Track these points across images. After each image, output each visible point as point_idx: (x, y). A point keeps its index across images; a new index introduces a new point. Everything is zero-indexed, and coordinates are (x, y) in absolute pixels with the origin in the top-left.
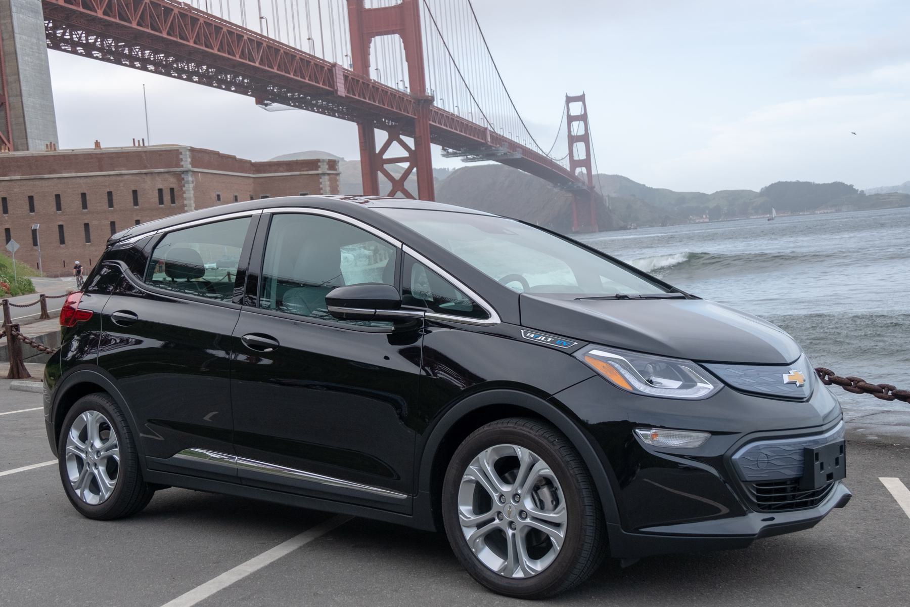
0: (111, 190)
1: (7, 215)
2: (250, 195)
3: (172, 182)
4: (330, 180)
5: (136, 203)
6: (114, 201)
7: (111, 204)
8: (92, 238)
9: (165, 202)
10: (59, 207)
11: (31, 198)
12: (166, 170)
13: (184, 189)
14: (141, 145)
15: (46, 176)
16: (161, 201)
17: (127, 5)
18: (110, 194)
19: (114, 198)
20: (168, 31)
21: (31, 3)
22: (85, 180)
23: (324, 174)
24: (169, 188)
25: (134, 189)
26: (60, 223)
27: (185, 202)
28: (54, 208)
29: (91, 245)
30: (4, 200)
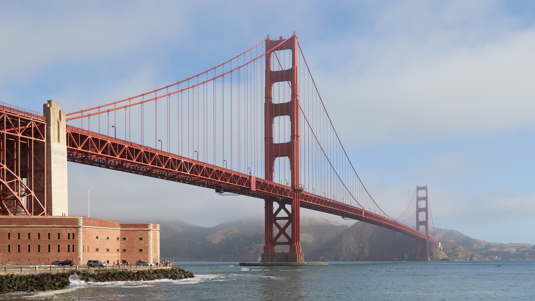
3: (74, 231)
4: (153, 233)
5: (59, 238)
6: (50, 237)
7: (49, 238)
8: (40, 250)
10: (29, 239)
11: (19, 234)
14: (64, 215)
16: (69, 238)
18: (49, 234)
19: (50, 235)
26: (29, 244)
27: (78, 239)
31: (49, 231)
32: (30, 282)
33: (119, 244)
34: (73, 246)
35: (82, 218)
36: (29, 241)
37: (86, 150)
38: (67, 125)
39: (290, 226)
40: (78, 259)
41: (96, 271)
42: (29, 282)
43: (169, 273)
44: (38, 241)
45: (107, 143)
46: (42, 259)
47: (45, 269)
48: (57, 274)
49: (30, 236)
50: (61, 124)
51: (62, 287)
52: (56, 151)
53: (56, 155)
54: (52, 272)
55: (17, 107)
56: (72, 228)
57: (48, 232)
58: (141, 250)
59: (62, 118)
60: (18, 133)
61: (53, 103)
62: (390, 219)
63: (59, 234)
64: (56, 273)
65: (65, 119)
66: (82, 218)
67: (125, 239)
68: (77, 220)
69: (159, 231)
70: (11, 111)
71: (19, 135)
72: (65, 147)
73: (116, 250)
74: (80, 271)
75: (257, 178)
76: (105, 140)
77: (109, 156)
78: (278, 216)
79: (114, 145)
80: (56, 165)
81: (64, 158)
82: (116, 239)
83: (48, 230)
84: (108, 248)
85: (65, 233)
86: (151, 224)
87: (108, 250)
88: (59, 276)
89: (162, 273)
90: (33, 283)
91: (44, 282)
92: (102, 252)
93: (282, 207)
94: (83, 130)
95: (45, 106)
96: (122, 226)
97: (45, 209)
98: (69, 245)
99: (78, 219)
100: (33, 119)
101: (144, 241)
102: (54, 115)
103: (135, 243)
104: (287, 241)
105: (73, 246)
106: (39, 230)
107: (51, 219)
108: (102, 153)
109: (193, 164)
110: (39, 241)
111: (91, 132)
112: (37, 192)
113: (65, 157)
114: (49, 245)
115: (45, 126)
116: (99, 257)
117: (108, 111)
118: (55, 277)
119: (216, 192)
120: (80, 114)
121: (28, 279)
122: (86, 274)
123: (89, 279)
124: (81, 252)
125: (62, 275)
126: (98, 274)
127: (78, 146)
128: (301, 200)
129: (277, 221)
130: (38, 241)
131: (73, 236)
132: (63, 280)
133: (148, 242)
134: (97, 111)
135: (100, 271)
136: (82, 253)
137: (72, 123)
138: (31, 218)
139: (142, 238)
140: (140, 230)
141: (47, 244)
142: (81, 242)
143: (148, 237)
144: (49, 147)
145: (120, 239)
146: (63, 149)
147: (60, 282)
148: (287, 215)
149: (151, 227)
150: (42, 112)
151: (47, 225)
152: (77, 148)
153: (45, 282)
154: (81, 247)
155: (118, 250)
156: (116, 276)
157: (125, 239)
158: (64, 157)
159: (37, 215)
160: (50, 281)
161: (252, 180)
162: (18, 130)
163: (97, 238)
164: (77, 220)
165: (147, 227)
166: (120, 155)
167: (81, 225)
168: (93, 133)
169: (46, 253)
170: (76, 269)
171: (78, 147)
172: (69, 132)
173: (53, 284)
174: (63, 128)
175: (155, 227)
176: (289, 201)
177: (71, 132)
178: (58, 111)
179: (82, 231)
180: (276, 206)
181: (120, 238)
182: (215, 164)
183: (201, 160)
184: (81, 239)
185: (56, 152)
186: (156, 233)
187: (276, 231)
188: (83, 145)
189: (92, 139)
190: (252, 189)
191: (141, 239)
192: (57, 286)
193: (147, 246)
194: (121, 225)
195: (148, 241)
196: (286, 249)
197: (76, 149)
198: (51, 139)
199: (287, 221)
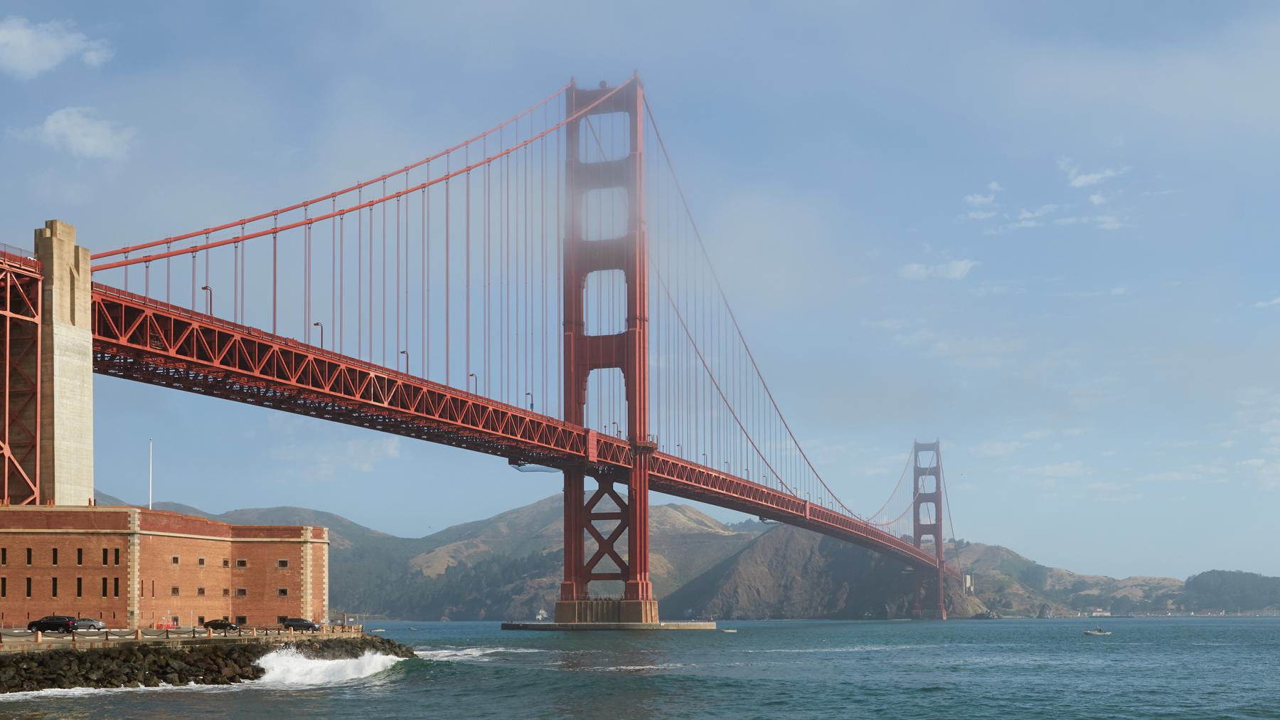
3: (117, 542)
5: (80, 562)
6: (58, 558)
7: (55, 562)
8: (32, 592)
9: (109, 562)
12: (112, 531)
13: (129, 550)
14: (93, 504)
16: (105, 562)
18: (55, 551)
19: (59, 555)
22: (32, 537)
23: (306, 542)
26: (4, 576)
29: (30, 600)
31: (55, 543)
32: (26, 673)
33: (229, 576)
34: (116, 580)
35: (139, 511)
36: (4, 568)
37: (139, 344)
38: (92, 283)
39: (625, 536)
40: (129, 615)
41: (184, 643)
42: (23, 672)
43: (360, 648)
44: (26, 568)
45: (191, 328)
46: (35, 613)
47: (58, 639)
48: (92, 651)
50: (78, 281)
51: (107, 683)
52: (67, 347)
54: (77, 645)
55: (3, 247)
56: (113, 537)
58: (283, 592)
59: (81, 265)
61: (59, 227)
62: (856, 519)
63: (80, 551)
64: (89, 647)
65: (90, 267)
66: (139, 511)
67: (242, 563)
68: (126, 515)
69: (329, 544)
70: (4, 261)
72: (90, 336)
73: (222, 592)
74: (148, 643)
75: (599, 434)
76: (186, 320)
77: (195, 359)
78: (594, 511)
79: (207, 332)
80: (65, 379)
81: (86, 364)
82: (221, 564)
84: (202, 586)
85: (95, 548)
86: (309, 528)
87: (201, 591)
88: (96, 657)
89: (344, 649)
90: (33, 673)
91: (61, 672)
92: (187, 596)
93: (606, 488)
94: (132, 295)
95: (39, 234)
96: (237, 531)
97: (36, 490)
98: (105, 580)
99: (129, 513)
100: (9, 265)
101: (290, 569)
102: (61, 258)
103: (268, 574)
104: (617, 570)
105: (116, 580)
106: (29, 542)
107: (49, 515)
108: (177, 352)
109: (422, 389)
110: (30, 568)
111: (151, 301)
112: (17, 447)
113: (88, 360)
114: (55, 580)
115: (40, 284)
116: (180, 609)
117: (194, 250)
118: (86, 660)
119: (510, 463)
120: (120, 258)
121: (20, 665)
122: (162, 651)
123: (170, 662)
124: (136, 596)
125: (104, 652)
126: (191, 651)
127: (119, 336)
128: (651, 473)
129: (594, 523)
130: (26, 568)
131: (116, 557)
132: (108, 667)
133: (302, 571)
134: (162, 249)
135: (196, 642)
136: (138, 599)
137: (105, 278)
138: (9, 511)
140: (281, 542)
141: (49, 575)
142: (136, 570)
143: (302, 560)
144: (49, 335)
145: (230, 565)
146: (82, 342)
147: (101, 672)
148: (617, 509)
149: (308, 535)
150: (32, 249)
151: (49, 528)
152: (117, 338)
153: (63, 670)
154: (136, 583)
155: (226, 592)
156: (235, 655)
157: (242, 563)
159: (18, 503)
160: (75, 668)
161: (590, 438)
163: (176, 560)
164: (126, 515)
165: (300, 535)
166: (221, 359)
167: (137, 529)
168: (156, 302)
169: (48, 599)
170: (136, 638)
171: (121, 338)
172: (98, 299)
173: (83, 675)
174: (85, 289)
175: (318, 535)
176: (623, 476)
177: (102, 300)
178: (73, 248)
179: (140, 544)
180: (591, 485)
181: (230, 561)
182: (545, 411)
183: (416, 372)
184: (136, 564)
185: (67, 349)
186: (322, 549)
187: (591, 546)
188: (131, 333)
189: (153, 317)
190: (590, 459)
191: (283, 564)
192: (94, 681)
193: (298, 581)
194: (233, 529)
195: (302, 568)
196: (615, 591)
197: (114, 341)
198: (54, 316)
199: (618, 522)
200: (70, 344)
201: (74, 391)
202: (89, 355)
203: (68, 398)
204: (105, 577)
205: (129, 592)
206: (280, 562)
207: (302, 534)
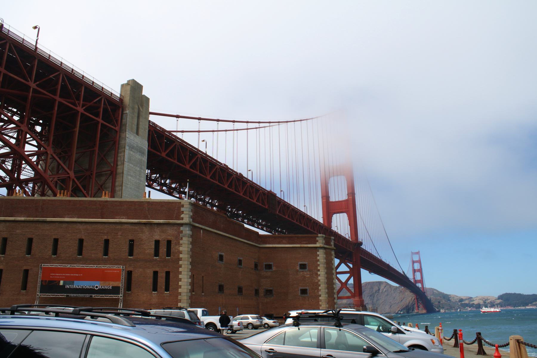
0: (108, 238)
1: (4, 255)
2: (255, 262)
5: (131, 253)
9: (160, 254)
11: (30, 241)
15: (49, 219)
16: (157, 254)
17: (206, 168)
18: (107, 242)
19: (110, 246)
20: (228, 185)
21: (140, 147)
22: (85, 226)
24: (166, 240)
25: (131, 239)
28: (50, 252)
30: (5, 240)
31: (107, 233)
34: (168, 274)
49: (59, 246)
53: (131, 150)
57: (106, 237)
60: (79, 106)
71: (81, 110)
80: (131, 165)
83: (105, 231)
87: (240, 290)
105: (168, 274)
113: (145, 157)
127: (161, 151)
133: (319, 273)
139: (306, 265)
158: (143, 157)
162: (79, 104)
163: (221, 258)
171: (162, 153)
177: (154, 130)
188: (168, 151)
191: (303, 267)
200: (135, 145)
201: (136, 173)
202: (145, 154)
203: (131, 176)
204: (157, 269)
205: (180, 287)
206: (301, 265)
207: (317, 241)
